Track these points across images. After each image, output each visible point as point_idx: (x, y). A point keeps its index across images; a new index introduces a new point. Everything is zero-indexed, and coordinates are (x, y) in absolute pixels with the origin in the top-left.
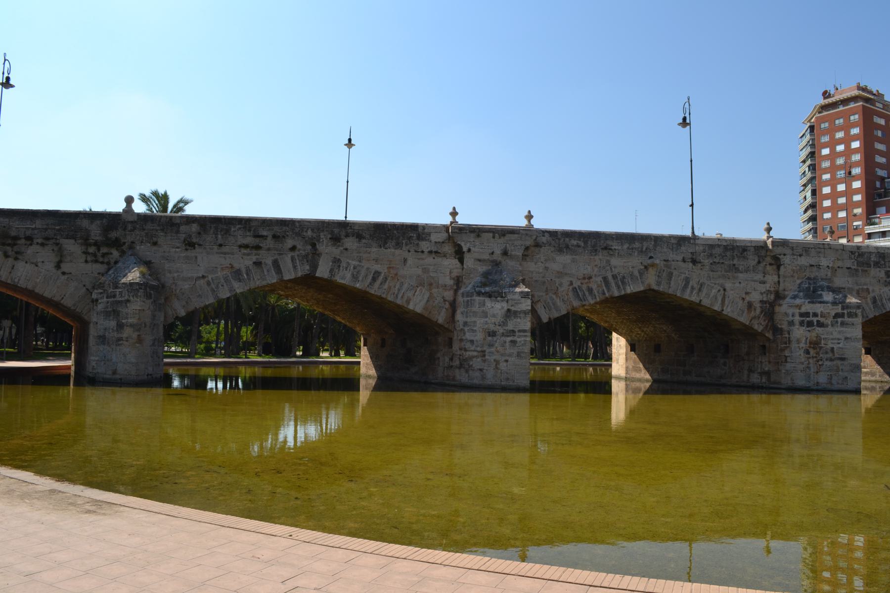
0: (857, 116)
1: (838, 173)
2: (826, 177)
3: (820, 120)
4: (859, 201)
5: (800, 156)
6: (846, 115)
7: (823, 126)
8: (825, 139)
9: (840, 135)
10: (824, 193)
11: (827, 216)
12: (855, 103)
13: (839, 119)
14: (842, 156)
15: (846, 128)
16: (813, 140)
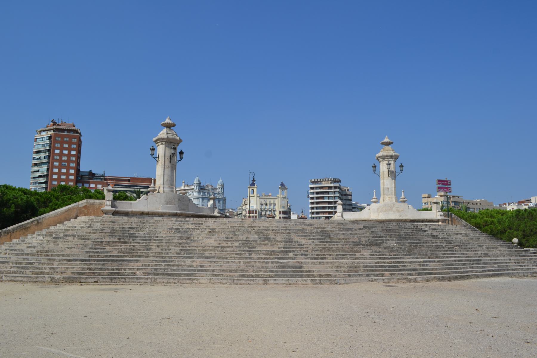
0: (76, 140)
1: (63, 164)
2: (56, 164)
3: (56, 136)
4: (73, 179)
5: (34, 148)
6: (71, 138)
7: (57, 139)
8: (59, 145)
9: (66, 146)
10: (54, 171)
11: (55, 183)
12: (74, 133)
13: (67, 138)
14: (66, 156)
15: (70, 143)
16: (50, 144)
